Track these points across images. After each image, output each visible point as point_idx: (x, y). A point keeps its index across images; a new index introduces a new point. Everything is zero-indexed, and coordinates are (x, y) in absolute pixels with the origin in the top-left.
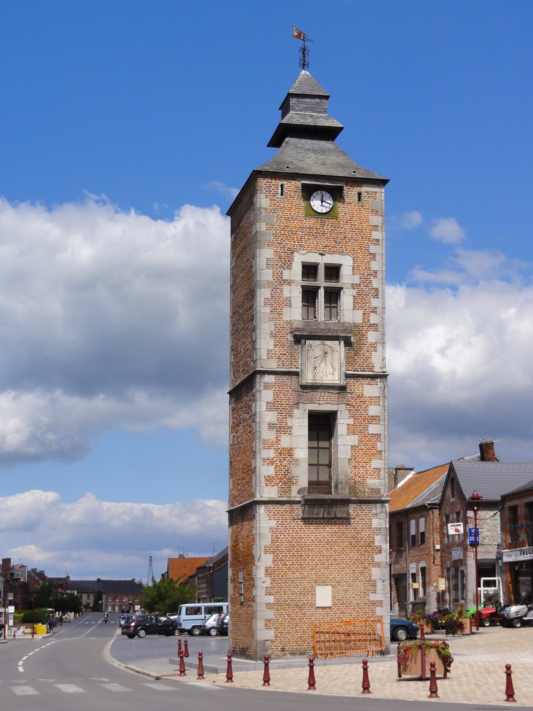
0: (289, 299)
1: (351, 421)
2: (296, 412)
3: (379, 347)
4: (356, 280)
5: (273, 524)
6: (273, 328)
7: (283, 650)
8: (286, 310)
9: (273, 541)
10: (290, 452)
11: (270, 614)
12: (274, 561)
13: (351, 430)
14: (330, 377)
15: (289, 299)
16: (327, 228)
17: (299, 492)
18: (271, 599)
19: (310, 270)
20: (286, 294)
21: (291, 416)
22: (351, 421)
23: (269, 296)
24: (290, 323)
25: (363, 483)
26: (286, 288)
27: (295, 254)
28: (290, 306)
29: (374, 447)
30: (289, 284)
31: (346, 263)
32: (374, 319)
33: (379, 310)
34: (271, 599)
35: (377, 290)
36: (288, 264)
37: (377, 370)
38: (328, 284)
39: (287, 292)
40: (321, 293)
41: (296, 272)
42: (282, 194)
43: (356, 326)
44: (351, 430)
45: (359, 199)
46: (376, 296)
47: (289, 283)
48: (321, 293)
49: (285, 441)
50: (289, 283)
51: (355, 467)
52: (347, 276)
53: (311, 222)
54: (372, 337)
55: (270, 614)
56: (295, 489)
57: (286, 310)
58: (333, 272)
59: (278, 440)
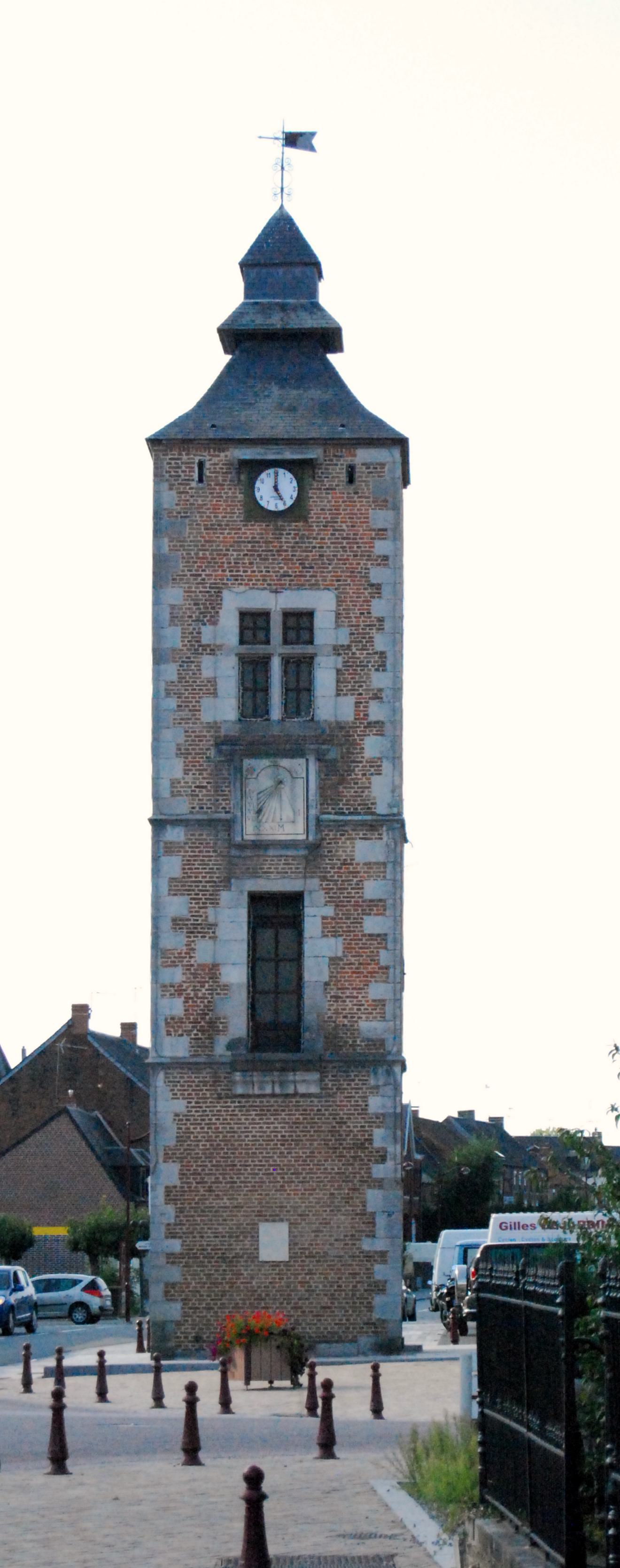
0: (213, 682)
1: (329, 911)
2: (225, 896)
3: (386, 766)
4: (343, 638)
5: (180, 1106)
6: (181, 739)
7: (197, 1339)
8: (207, 702)
9: (179, 1139)
10: (213, 970)
11: (175, 1274)
12: (182, 1174)
13: (330, 929)
14: (288, 828)
15: (213, 682)
16: (287, 540)
17: (230, 1046)
18: (176, 1246)
19: (253, 623)
20: (207, 673)
21: (215, 903)
22: (329, 911)
23: (175, 678)
24: (214, 726)
25: (353, 1030)
26: (206, 661)
27: (226, 594)
28: (215, 694)
29: (374, 959)
30: (213, 652)
31: (323, 604)
32: (376, 712)
33: (387, 695)
34: (176, 1246)
35: (382, 654)
36: (209, 611)
37: (381, 809)
38: (288, 650)
39: (207, 666)
40: (276, 665)
41: (228, 626)
42: (201, 480)
43: (340, 726)
44: (330, 929)
45: (351, 480)
46: (382, 667)
47: (213, 650)
48: (276, 665)
49: (204, 951)
50: (213, 650)
51: (336, 998)
52: (326, 630)
53: (255, 530)
54: (371, 746)
55: (175, 1274)
56: (222, 1042)
57: (207, 702)
58: (300, 624)
59: (191, 950)
